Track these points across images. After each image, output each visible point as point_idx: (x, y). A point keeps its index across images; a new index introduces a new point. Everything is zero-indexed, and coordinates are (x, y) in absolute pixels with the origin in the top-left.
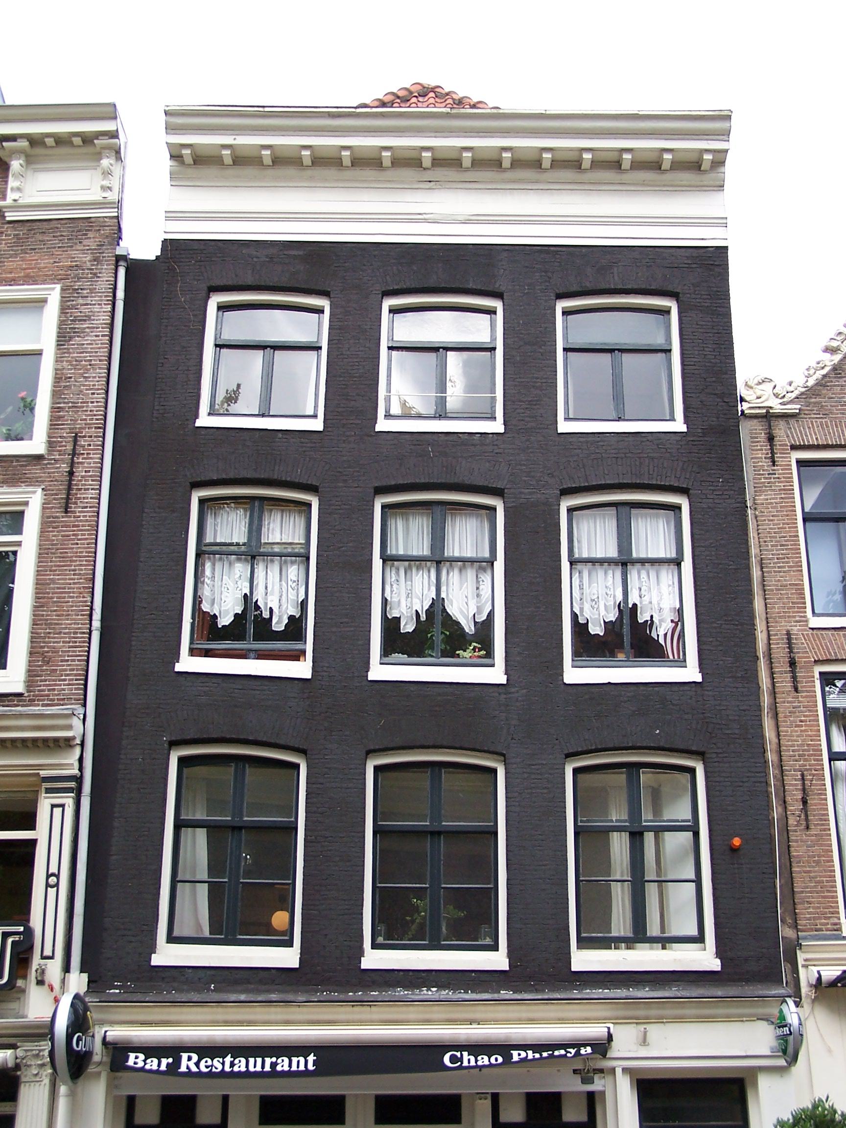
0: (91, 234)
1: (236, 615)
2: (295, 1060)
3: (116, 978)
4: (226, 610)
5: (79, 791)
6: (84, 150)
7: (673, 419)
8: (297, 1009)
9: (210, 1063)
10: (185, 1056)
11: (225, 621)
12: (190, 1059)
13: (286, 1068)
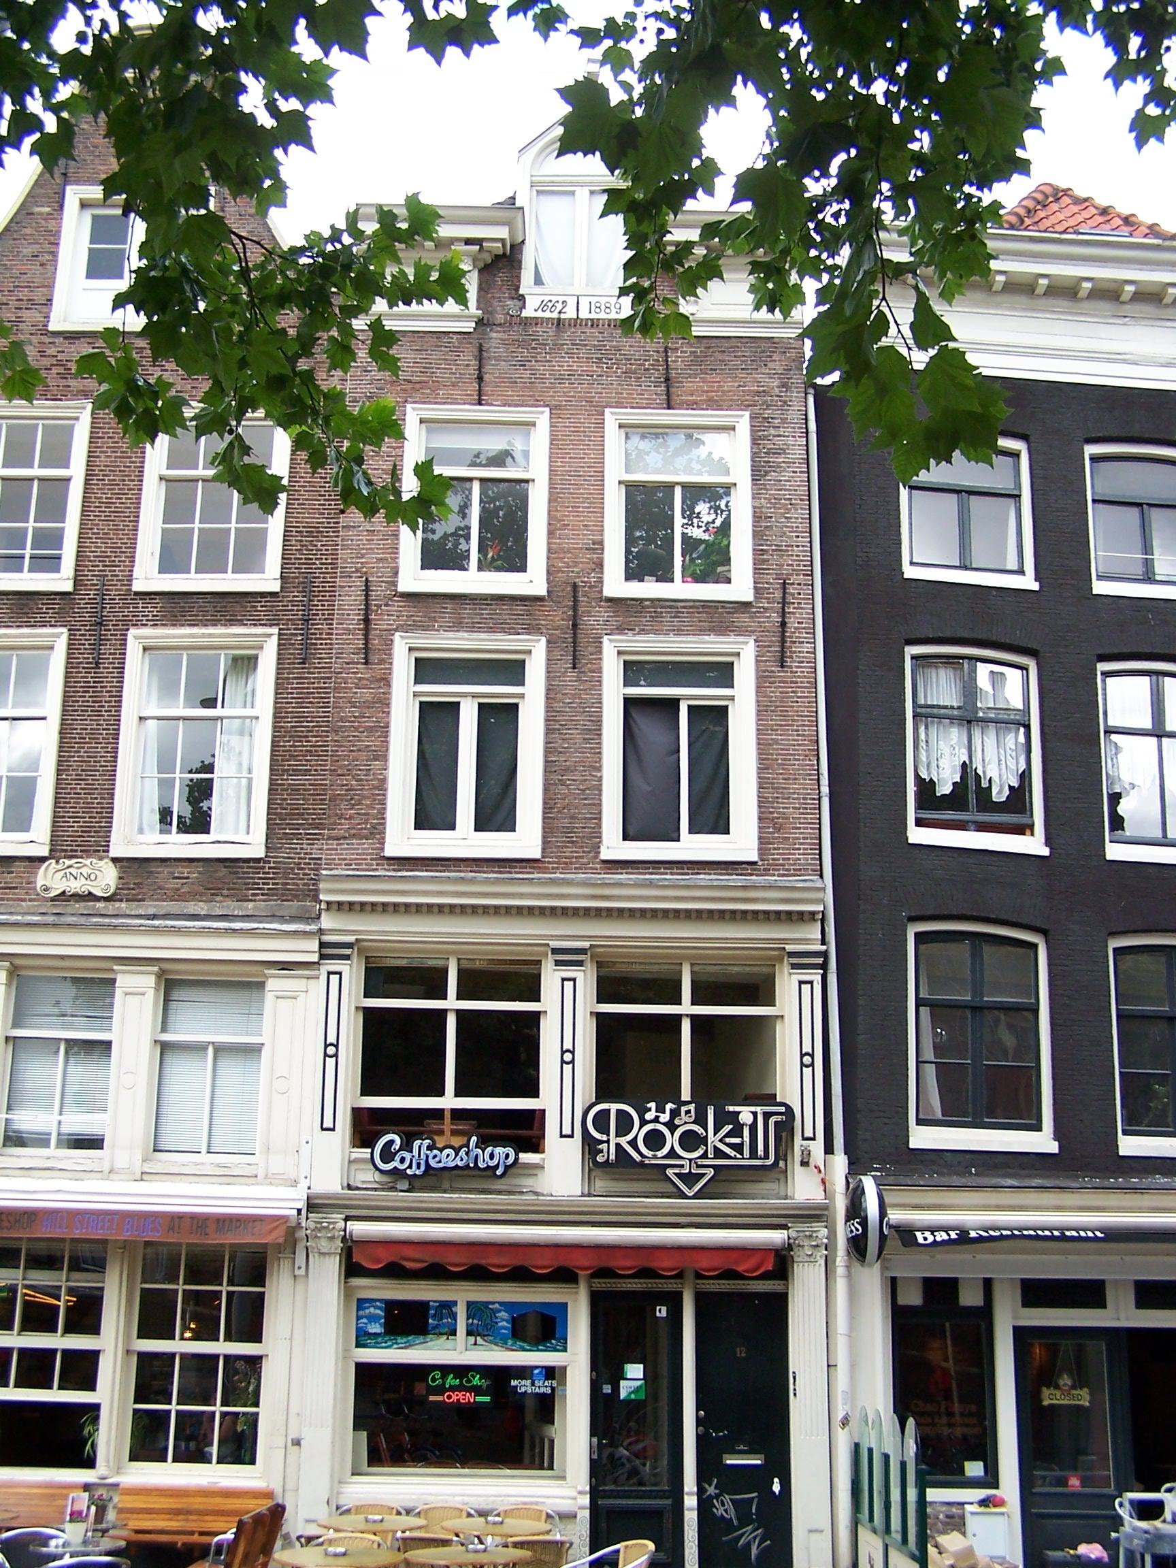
0: (776, 357)
3: (874, 1160)
5: (824, 966)
8: (1070, 1195)
11: (945, 789)
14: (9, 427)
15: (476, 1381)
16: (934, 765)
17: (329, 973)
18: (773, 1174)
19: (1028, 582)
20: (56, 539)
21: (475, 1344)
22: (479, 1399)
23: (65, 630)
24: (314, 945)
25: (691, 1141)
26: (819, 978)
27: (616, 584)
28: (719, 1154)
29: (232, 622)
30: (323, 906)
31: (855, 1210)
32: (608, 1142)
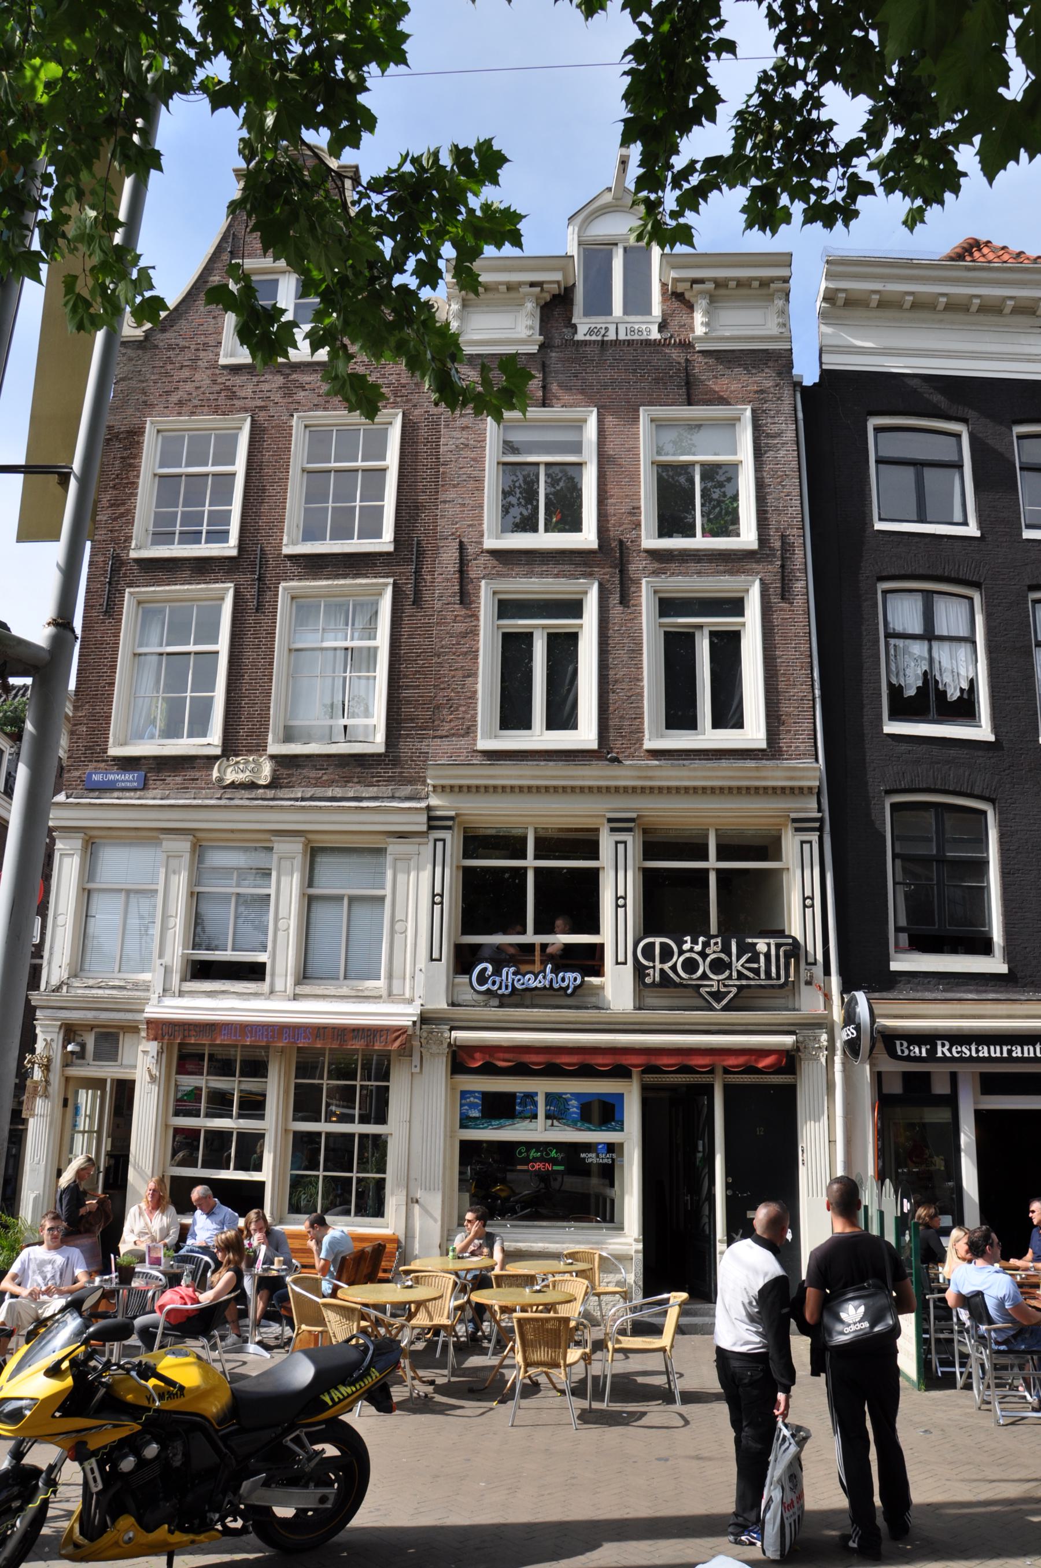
0: (770, 364)
1: (918, 688)
2: (1026, 1048)
4: (912, 684)
5: (820, 829)
6: (759, 292)
7: (965, 523)
9: (959, 1049)
10: (939, 1043)
11: (911, 692)
12: (902, 1045)
13: (1020, 1055)
14: (190, 437)
15: (553, 1154)
16: (901, 674)
17: (436, 840)
18: (783, 991)
19: (972, 530)
20: (226, 517)
21: (552, 1125)
22: (556, 1168)
23: (232, 585)
24: (424, 818)
25: (718, 966)
26: (817, 838)
27: (650, 541)
28: (741, 976)
29: (357, 576)
30: (431, 788)
31: (850, 1018)
32: (654, 967)
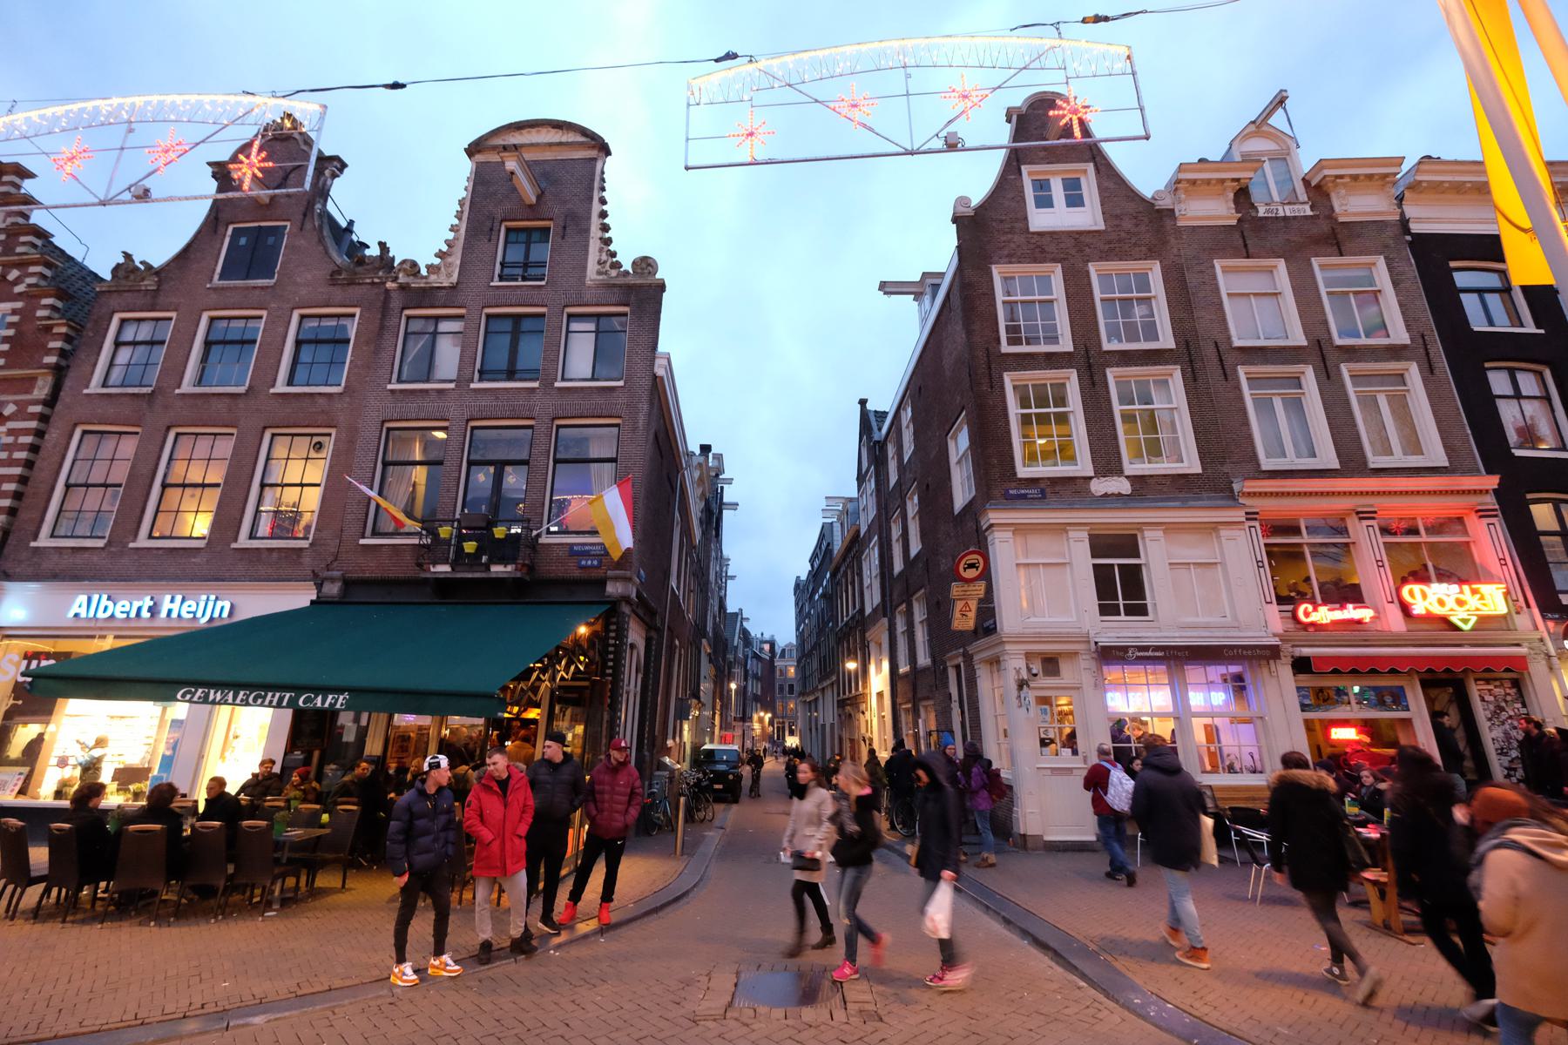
25: (1460, 603)
